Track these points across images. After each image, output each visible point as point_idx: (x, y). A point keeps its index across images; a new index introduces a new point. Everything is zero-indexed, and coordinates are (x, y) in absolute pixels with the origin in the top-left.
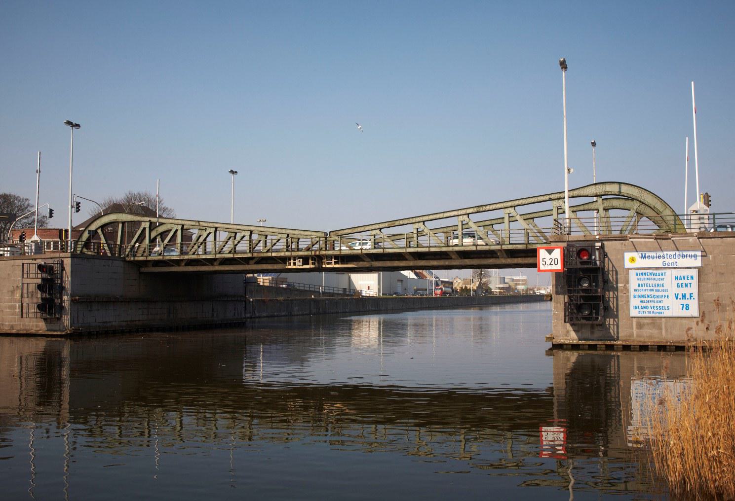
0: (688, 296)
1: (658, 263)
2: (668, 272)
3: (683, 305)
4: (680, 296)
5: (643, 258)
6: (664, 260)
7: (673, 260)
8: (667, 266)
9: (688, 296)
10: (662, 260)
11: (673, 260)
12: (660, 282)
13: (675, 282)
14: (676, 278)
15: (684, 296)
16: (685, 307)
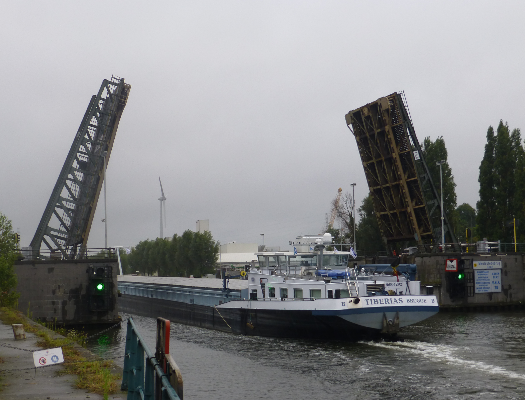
0: (497, 282)
1: (485, 267)
2: (490, 271)
3: (495, 286)
4: (494, 282)
5: (480, 264)
6: (488, 265)
7: (491, 265)
8: (488, 268)
9: (497, 282)
10: (487, 265)
11: (491, 265)
12: (487, 276)
13: (492, 276)
14: (493, 274)
15: (496, 282)
16: (496, 288)
